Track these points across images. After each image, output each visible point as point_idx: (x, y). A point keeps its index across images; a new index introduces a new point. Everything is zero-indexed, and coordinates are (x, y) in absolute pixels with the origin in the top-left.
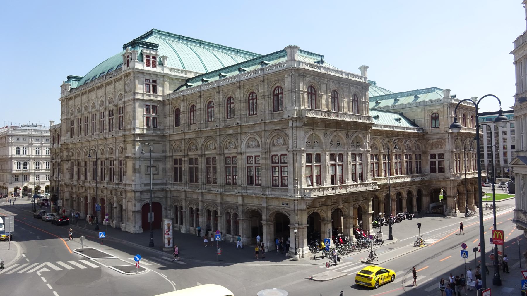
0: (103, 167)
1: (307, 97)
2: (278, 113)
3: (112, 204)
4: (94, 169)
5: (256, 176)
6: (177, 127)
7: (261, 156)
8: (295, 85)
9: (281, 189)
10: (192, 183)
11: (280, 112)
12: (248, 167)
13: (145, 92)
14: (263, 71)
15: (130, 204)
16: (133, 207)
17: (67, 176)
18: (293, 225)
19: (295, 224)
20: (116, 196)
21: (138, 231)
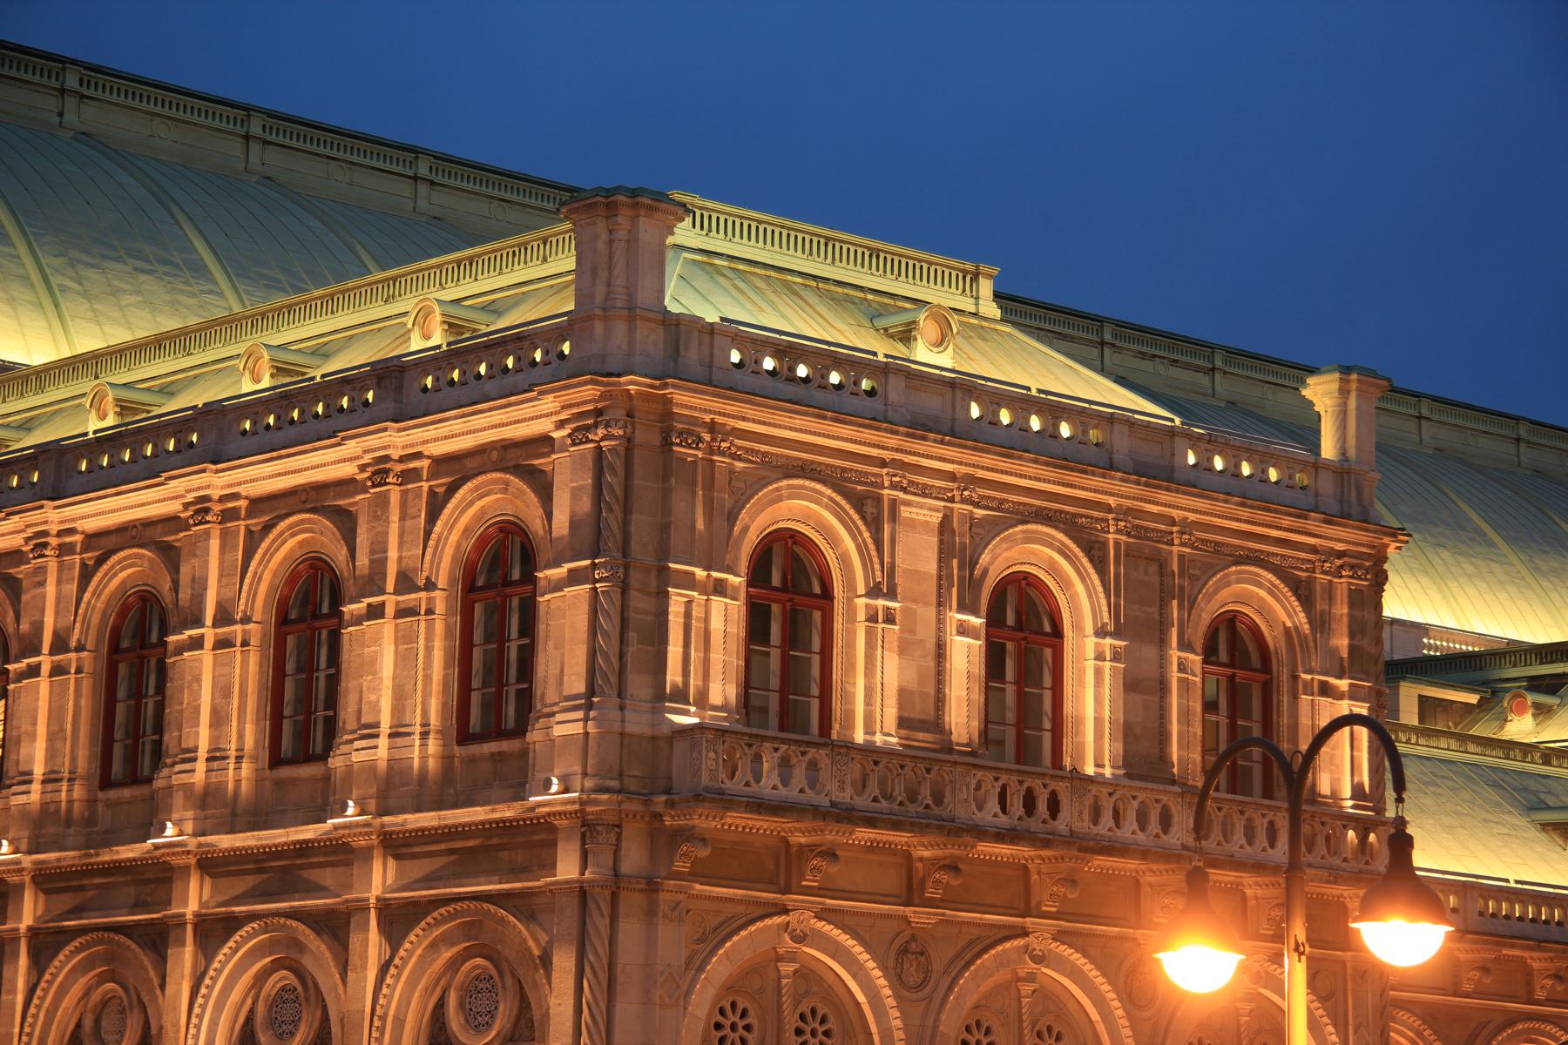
1: (738, 629)
2: (498, 757)
8: (625, 525)
11: (505, 745)
14: (399, 389)
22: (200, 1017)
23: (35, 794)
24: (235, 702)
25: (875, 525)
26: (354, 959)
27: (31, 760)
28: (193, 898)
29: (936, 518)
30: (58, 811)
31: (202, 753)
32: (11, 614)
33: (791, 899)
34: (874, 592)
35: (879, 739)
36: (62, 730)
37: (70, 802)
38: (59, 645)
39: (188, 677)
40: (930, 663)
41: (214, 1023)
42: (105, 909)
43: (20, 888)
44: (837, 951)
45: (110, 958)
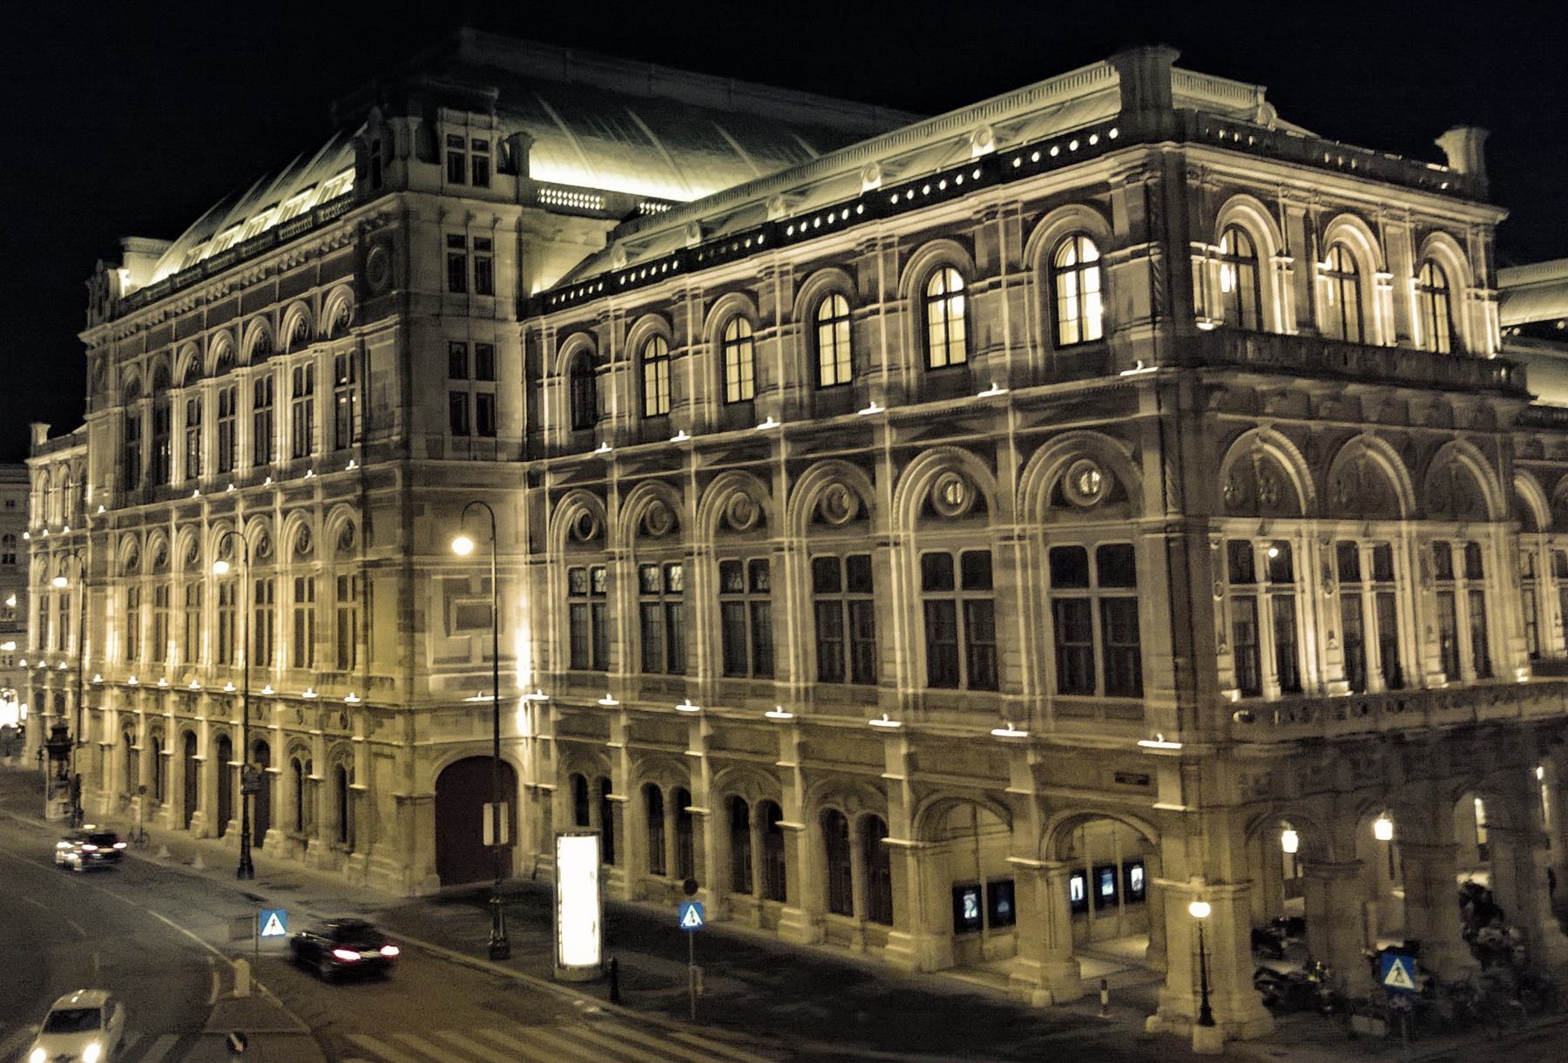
0: (265, 608)
3: (303, 763)
4: (222, 616)
5: (970, 647)
6: (581, 433)
7: (995, 556)
9: (1107, 706)
10: (657, 676)
12: (926, 603)
13: (446, 286)
15: (384, 766)
16: (404, 782)
17: (114, 648)
18: (1181, 880)
19: (1192, 875)
20: (321, 729)
21: (420, 884)
22: (900, 499)
23: (780, 395)
24: (902, 340)
25: (1277, 217)
26: (1001, 463)
27: (776, 377)
28: (888, 440)
29: (1303, 212)
30: (794, 404)
31: (885, 367)
32: (753, 308)
33: (1259, 419)
34: (1280, 254)
35: (1289, 332)
36: (792, 362)
37: (801, 398)
38: (786, 320)
39: (871, 330)
40: (1305, 291)
41: (908, 501)
42: (828, 448)
43: (778, 440)
44: (1280, 447)
45: (836, 472)
